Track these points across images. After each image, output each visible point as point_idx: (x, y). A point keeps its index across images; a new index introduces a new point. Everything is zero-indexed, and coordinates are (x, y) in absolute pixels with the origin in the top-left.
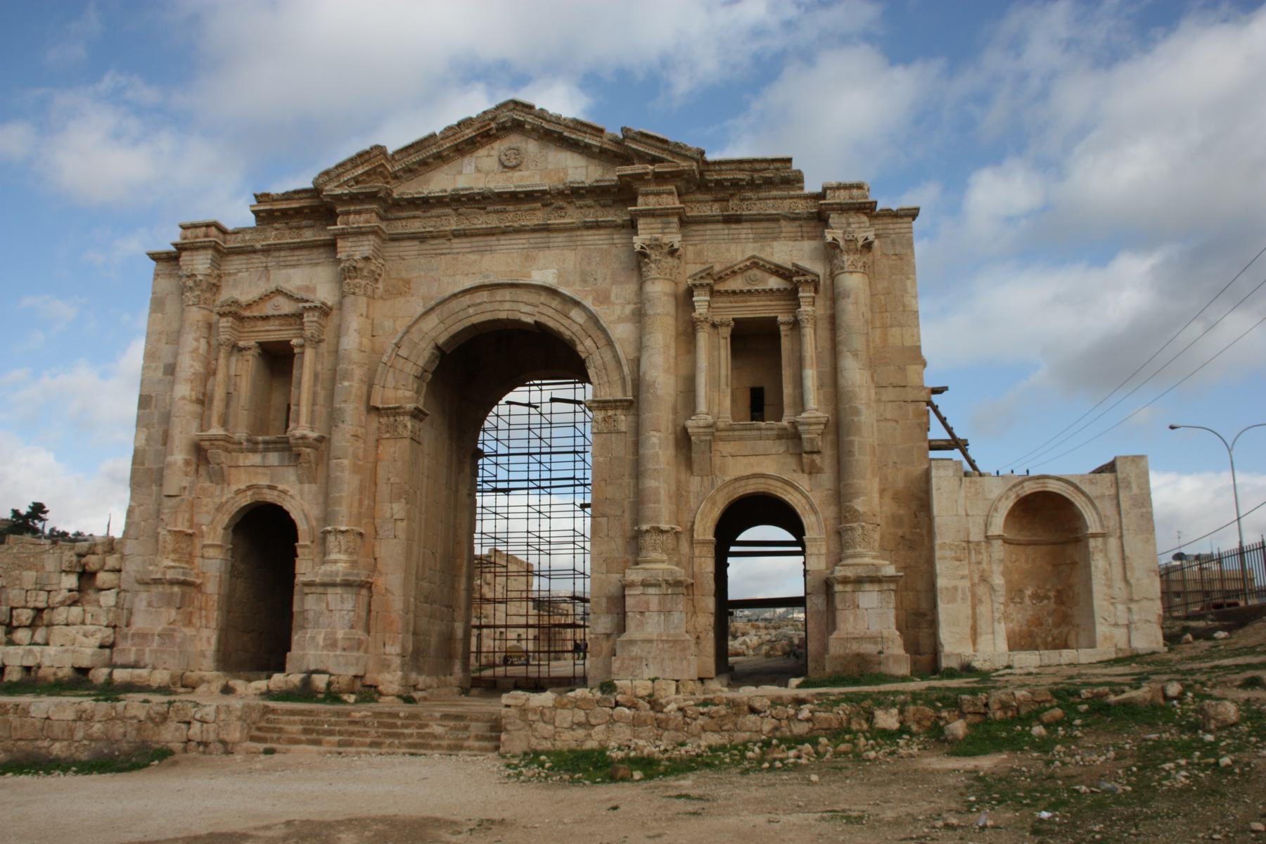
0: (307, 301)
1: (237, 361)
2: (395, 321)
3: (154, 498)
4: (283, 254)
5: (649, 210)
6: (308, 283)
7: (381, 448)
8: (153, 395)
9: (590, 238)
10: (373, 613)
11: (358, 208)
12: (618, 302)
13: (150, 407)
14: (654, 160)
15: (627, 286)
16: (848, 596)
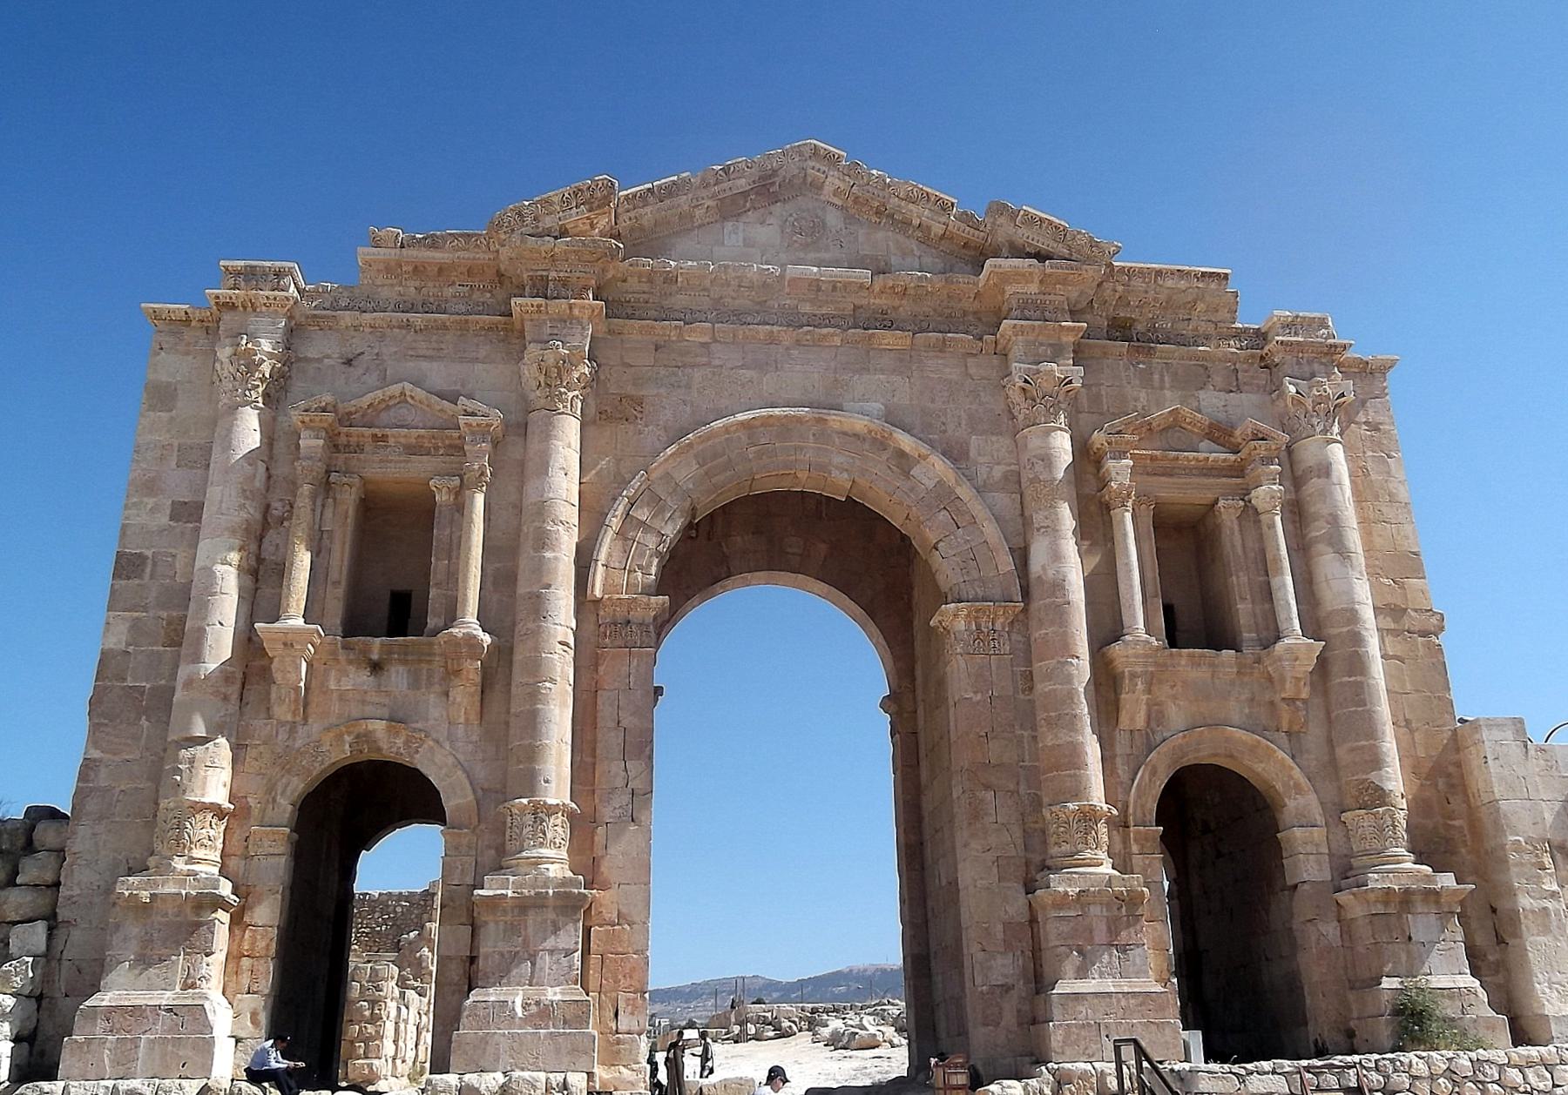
0: (473, 414)
1: (323, 506)
2: (618, 461)
3: (143, 742)
4: (411, 336)
5: (1033, 328)
6: (458, 387)
7: (601, 669)
8: (149, 553)
9: (930, 362)
10: (594, 958)
11: (561, 274)
12: (981, 459)
13: (140, 577)
14: (1041, 257)
15: (994, 438)
16: (1393, 920)
